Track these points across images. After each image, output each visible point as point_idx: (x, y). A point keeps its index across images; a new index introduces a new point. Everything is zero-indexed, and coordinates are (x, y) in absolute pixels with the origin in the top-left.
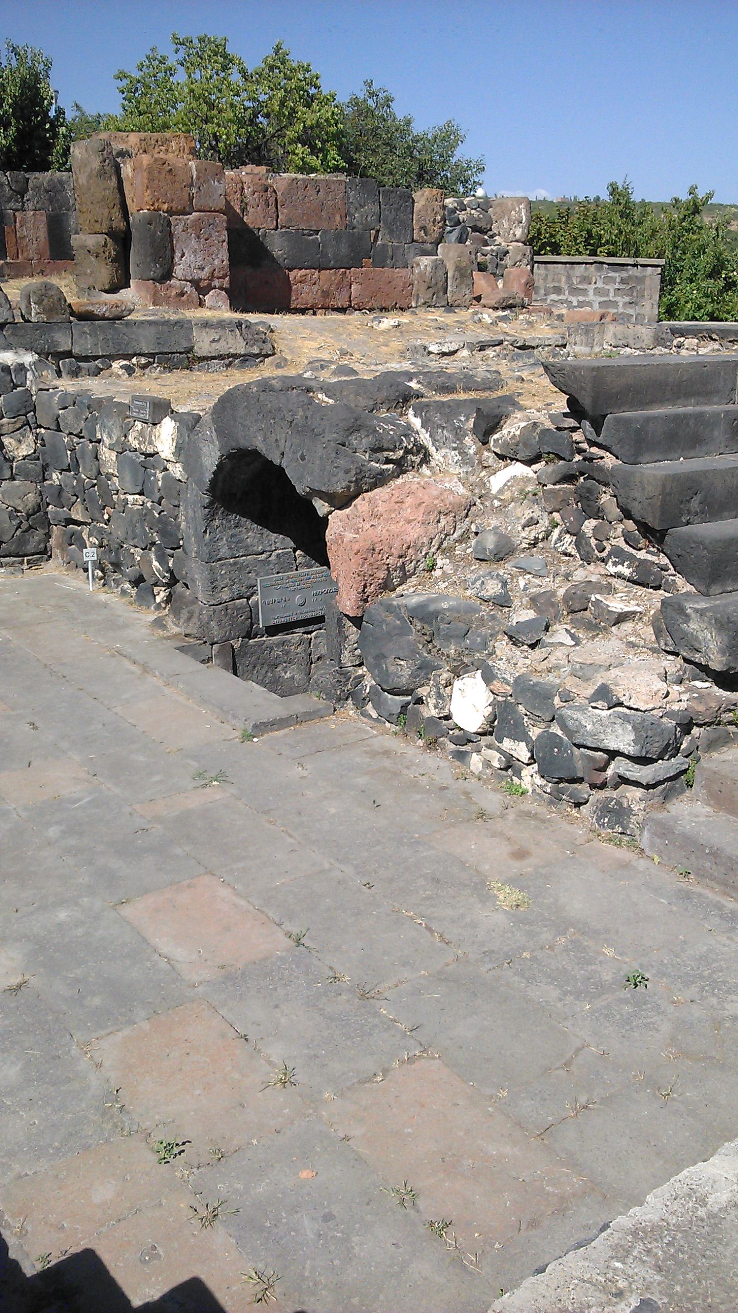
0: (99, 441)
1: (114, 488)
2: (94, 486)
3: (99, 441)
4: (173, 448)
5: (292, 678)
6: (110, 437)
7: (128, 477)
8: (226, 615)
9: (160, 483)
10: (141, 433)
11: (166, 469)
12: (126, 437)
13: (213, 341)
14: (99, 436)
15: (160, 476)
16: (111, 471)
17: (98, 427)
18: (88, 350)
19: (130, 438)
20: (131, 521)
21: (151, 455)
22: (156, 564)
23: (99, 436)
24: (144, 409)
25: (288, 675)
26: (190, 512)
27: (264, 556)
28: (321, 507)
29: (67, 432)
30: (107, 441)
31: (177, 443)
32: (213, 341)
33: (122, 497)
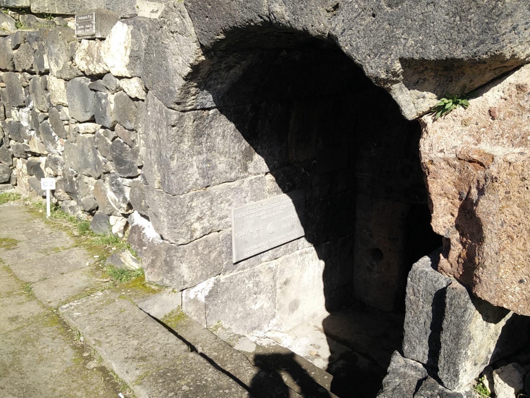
0: (47, 72)
1: (64, 117)
2: (46, 118)
3: (47, 72)
4: (127, 60)
5: (261, 308)
6: (57, 63)
7: (78, 104)
8: (197, 254)
9: (112, 106)
10: (89, 52)
11: (119, 89)
12: (72, 59)
13: (153, 12)
14: (46, 66)
15: (111, 98)
16: (61, 101)
17: (45, 57)
18: (45, 8)
19: (77, 60)
20: (83, 151)
21: (100, 76)
22: (111, 195)
23: (46, 66)
24: (89, 22)
25: (258, 306)
26: (153, 135)
27: (236, 184)
28: (412, 102)
29: (20, 70)
30: (54, 69)
31: (132, 51)
32: (153, 12)
33: (74, 126)
